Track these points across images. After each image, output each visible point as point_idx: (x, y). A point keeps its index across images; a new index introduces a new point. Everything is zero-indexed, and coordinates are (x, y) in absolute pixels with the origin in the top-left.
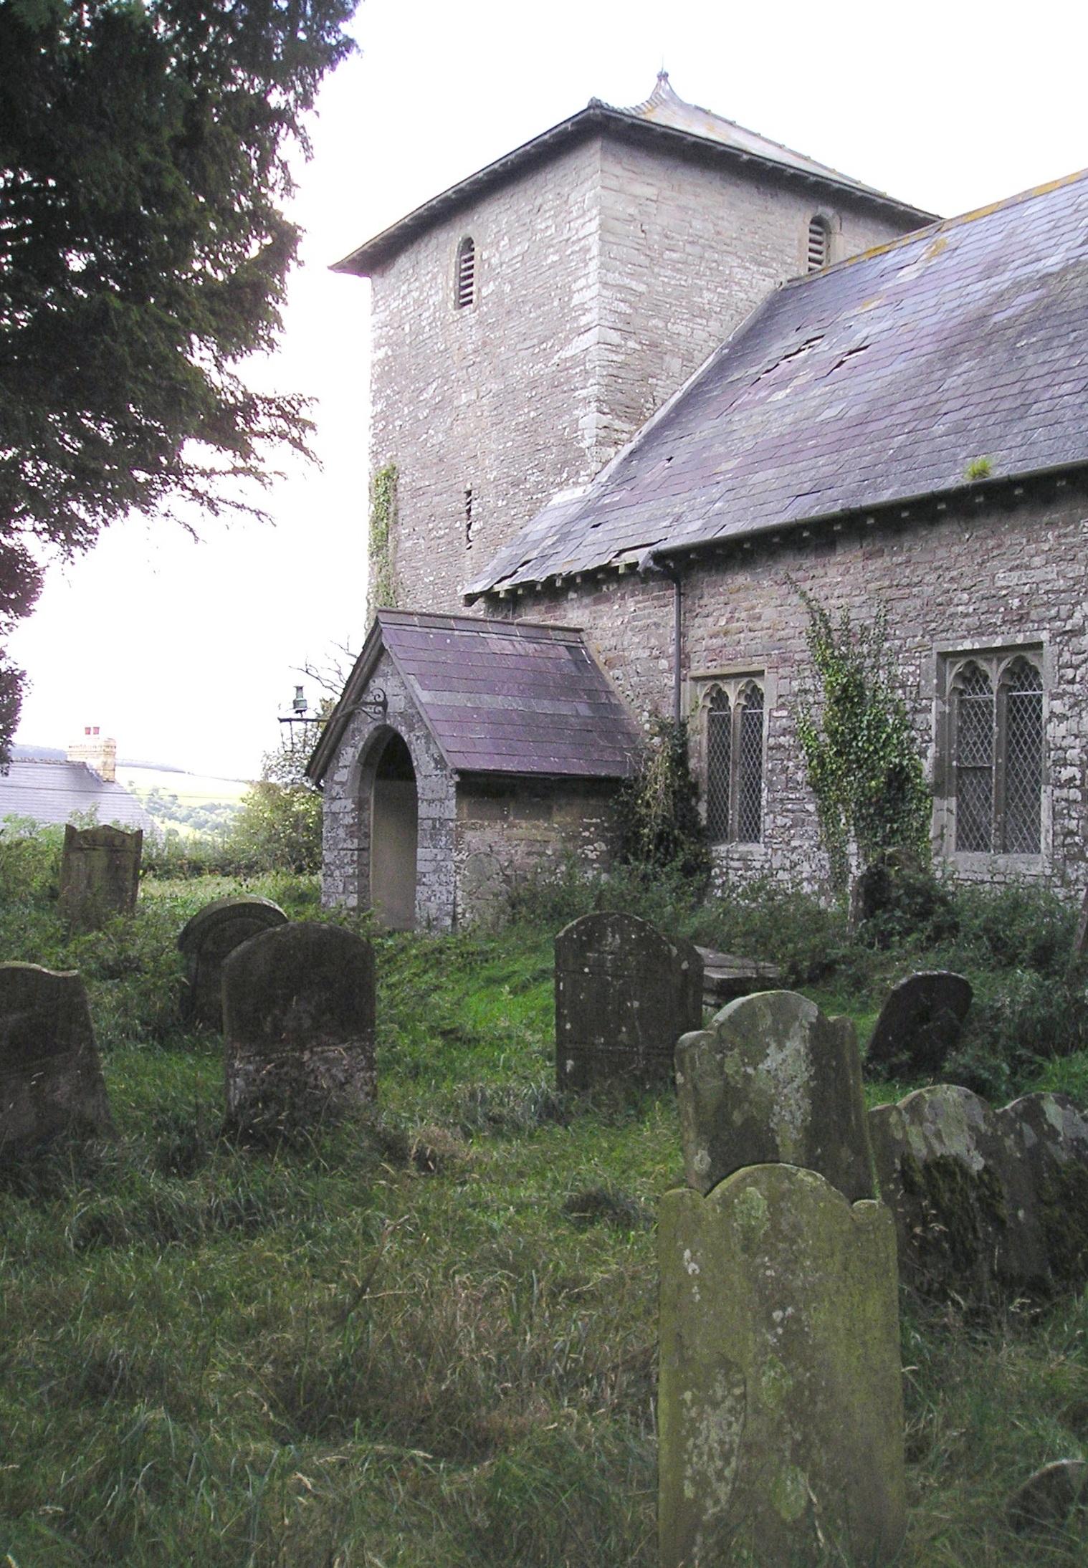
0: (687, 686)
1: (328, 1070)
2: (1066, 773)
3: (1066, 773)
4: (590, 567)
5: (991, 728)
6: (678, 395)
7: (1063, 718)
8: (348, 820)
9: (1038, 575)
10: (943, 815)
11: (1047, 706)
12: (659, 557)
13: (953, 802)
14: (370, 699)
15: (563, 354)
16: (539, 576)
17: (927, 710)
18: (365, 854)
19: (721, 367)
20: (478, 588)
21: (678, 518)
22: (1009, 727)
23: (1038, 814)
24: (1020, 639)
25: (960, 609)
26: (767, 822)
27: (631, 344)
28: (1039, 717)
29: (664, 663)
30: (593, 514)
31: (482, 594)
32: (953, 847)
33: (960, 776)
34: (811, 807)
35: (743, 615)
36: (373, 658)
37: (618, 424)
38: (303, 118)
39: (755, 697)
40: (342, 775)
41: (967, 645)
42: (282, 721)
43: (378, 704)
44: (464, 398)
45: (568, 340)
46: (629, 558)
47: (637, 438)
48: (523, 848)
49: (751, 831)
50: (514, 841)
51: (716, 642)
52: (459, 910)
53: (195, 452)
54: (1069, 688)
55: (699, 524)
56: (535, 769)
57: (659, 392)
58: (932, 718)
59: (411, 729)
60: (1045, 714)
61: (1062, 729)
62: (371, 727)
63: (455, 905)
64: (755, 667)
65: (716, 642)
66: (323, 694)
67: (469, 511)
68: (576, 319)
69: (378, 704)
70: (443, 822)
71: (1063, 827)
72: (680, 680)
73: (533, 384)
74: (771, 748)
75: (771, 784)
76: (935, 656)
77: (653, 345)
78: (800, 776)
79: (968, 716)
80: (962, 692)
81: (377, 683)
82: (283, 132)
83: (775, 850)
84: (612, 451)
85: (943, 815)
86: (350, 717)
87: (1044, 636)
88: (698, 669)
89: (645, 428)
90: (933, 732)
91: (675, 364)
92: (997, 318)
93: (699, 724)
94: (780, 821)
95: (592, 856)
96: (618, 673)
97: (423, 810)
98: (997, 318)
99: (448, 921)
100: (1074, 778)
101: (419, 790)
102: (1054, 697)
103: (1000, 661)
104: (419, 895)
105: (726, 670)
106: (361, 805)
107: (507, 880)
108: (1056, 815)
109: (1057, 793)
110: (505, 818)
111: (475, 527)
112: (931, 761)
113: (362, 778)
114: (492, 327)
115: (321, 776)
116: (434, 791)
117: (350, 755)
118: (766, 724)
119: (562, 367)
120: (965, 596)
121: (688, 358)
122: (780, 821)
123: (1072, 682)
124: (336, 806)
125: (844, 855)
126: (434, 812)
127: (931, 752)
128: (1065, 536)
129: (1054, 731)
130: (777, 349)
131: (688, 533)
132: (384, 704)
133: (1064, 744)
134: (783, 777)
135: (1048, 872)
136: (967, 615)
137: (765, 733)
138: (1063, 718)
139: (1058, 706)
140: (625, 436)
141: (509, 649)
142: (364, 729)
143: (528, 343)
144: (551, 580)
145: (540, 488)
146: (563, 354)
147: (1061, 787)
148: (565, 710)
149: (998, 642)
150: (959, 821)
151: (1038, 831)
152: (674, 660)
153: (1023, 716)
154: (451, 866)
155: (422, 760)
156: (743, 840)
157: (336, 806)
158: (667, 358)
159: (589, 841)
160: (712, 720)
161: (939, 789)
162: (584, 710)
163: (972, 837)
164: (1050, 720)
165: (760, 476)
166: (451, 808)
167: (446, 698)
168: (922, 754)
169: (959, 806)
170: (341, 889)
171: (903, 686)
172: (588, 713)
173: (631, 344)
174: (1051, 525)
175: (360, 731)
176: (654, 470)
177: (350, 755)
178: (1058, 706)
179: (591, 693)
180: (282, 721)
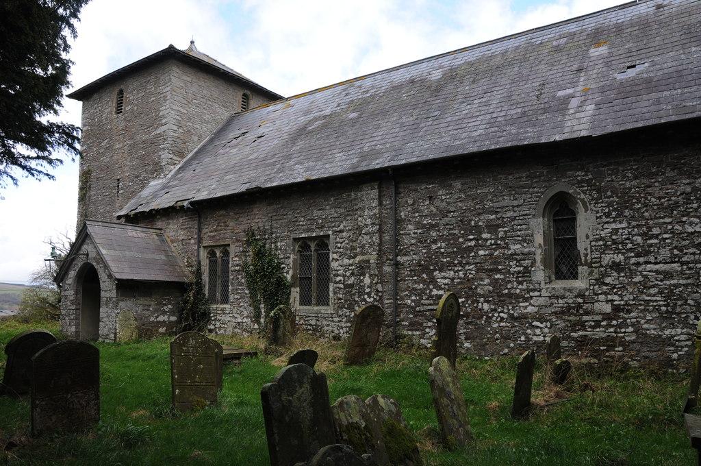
0: (202, 249)
1: (79, 401)
2: (338, 279)
3: (338, 279)
4: (166, 206)
5: (311, 264)
6: (196, 149)
7: (337, 260)
8: (72, 298)
9: (328, 212)
10: (295, 293)
11: (332, 256)
12: (192, 203)
13: (298, 289)
14: (81, 252)
15: (155, 132)
16: (147, 209)
17: (289, 257)
18: (78, 311)
19: (211, 141)
20: (123, 213)
21: (199, 190)
22: (318, 263)
23: (328, 293)
24: (322, 234)
25: (301, 223)
26: (231, 297)
27: (181, 130)
28: (328, 260)
29: (193, 241)
30: (166, 188)
31: (124, 216)
32: (298, 302)
33: (300, 280)
34: (247, 292)
35: (222, 224)
36: (83, 234)
37: (175, 158)
38: (73, 21)
39: (226, 253)
40: (69, 281)
41: (303, 235)
42: (46, 260)
43: (84, 254)
44: (118, 146)
45: (158, 127)
46: (180, 204)
47: (182, 163)
48: (141, 308)
49: (225, 300)
50: (132, 307)
51: (212, 234)
52: (118, 331)
53: (21, 149)
54: (339, 250)
55: (206, 193)
56: (146, 279)
57: (190, 148)
58: (291, 261)
59: (98, 264)
60: (331, 259)
61: (337, 264)
62: (82, 263)
63: (116, 329)
64: (226, 243)
65: (212, 234)
66: (64, 249)
67: (118, 186)
68: (161, 120)
69: (84, 254)
70: (111, 298)
71: (337, 297)
72: (199, 247)
73: (144, 142)
74: (232, 271)
75: (232, 284)
76: (292, 239)
77: (188, 131)
78: (243, 281)
79: (304, 260)
80: (301, 252)
81: (85, 247)
82: (63, 26)
83: (234, 307)
84: (172, 167)
85: (295, 293)
86: (73, 259)
87: (330, 233)
88: (205, 243)
89: (185, 160)
90: (291, 266)
91: (195, 138)
92: (310, 128)
93: (205, 263)
94: (236, 296)
95: (167, 310)
96: (175, 244)
97: (103, 294)
98: (310, 128)
99: (112, 335)
100: (341, 280)
101: (101, 287)
102: (334, 253)
103: (314, 241)
104: (101, 326)
105: (218, 244)
106: (76, 293)
107: (136, 319)
108: (335, 293)
109: (335, 285)
110: (135, 297)
111: (121, 192)
112: (290, 275)
113: (78, 282)
114: (129, 121)
115: (61, 281)
116: (107, 290)
117: (72, 274)
118: (231, 263)
119: (156, 136)
120: (303, 219)
121: (200, 137)
122: (236, 296)
123: (340, 248)
124: (67, 293)
125: (260, 308)
126: (107, 295)
127: (291, 272)
128: (338, 199)
129: (334, 265)
130: (232, 135)
131: (203, 195)
132: (87, 255)
133: (338, 268)
134: (237, 281)
135: (333, 312)
136: (303, 225)
137: (230, 266)
138: (337, 260)
139: (335, 256)
140: (177, 162)
141: (135, 235)
142: (79, 263)
143: (143, 128)
144: (151, 211)
145: (145, 179)
146: (155, 132)
147: (336, 283)
148: (157, 257)
149: (314, 235)
150: (300, 296)
151: (328, 299)
152: (197, 241)
153: (324, 262)
154: (114, 315)
155: (102, 276)
156: (221, 303)
157: (67, 293)
158: (193, 136)
159: (165, 305)
160: (210, 261)
161: (293, 285)
162: (163, 257)
163: (305, 300)
164: (332, 261)
165: (228, 177)
166: (114, 294)
167: (112, 252)
168: (287, 273)
169: (300, 291)
170: (68, 324)
171: (280, 249)
172: (165, 258)
173: (181, 130)
174: (333, 196)
175: (77, 264)
176: (188, 174)
177: (72, 274)
178: (335, 256)
179: (166, 251)
180: (46, 260)
